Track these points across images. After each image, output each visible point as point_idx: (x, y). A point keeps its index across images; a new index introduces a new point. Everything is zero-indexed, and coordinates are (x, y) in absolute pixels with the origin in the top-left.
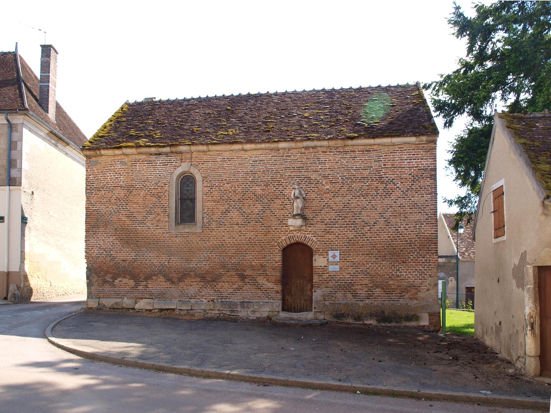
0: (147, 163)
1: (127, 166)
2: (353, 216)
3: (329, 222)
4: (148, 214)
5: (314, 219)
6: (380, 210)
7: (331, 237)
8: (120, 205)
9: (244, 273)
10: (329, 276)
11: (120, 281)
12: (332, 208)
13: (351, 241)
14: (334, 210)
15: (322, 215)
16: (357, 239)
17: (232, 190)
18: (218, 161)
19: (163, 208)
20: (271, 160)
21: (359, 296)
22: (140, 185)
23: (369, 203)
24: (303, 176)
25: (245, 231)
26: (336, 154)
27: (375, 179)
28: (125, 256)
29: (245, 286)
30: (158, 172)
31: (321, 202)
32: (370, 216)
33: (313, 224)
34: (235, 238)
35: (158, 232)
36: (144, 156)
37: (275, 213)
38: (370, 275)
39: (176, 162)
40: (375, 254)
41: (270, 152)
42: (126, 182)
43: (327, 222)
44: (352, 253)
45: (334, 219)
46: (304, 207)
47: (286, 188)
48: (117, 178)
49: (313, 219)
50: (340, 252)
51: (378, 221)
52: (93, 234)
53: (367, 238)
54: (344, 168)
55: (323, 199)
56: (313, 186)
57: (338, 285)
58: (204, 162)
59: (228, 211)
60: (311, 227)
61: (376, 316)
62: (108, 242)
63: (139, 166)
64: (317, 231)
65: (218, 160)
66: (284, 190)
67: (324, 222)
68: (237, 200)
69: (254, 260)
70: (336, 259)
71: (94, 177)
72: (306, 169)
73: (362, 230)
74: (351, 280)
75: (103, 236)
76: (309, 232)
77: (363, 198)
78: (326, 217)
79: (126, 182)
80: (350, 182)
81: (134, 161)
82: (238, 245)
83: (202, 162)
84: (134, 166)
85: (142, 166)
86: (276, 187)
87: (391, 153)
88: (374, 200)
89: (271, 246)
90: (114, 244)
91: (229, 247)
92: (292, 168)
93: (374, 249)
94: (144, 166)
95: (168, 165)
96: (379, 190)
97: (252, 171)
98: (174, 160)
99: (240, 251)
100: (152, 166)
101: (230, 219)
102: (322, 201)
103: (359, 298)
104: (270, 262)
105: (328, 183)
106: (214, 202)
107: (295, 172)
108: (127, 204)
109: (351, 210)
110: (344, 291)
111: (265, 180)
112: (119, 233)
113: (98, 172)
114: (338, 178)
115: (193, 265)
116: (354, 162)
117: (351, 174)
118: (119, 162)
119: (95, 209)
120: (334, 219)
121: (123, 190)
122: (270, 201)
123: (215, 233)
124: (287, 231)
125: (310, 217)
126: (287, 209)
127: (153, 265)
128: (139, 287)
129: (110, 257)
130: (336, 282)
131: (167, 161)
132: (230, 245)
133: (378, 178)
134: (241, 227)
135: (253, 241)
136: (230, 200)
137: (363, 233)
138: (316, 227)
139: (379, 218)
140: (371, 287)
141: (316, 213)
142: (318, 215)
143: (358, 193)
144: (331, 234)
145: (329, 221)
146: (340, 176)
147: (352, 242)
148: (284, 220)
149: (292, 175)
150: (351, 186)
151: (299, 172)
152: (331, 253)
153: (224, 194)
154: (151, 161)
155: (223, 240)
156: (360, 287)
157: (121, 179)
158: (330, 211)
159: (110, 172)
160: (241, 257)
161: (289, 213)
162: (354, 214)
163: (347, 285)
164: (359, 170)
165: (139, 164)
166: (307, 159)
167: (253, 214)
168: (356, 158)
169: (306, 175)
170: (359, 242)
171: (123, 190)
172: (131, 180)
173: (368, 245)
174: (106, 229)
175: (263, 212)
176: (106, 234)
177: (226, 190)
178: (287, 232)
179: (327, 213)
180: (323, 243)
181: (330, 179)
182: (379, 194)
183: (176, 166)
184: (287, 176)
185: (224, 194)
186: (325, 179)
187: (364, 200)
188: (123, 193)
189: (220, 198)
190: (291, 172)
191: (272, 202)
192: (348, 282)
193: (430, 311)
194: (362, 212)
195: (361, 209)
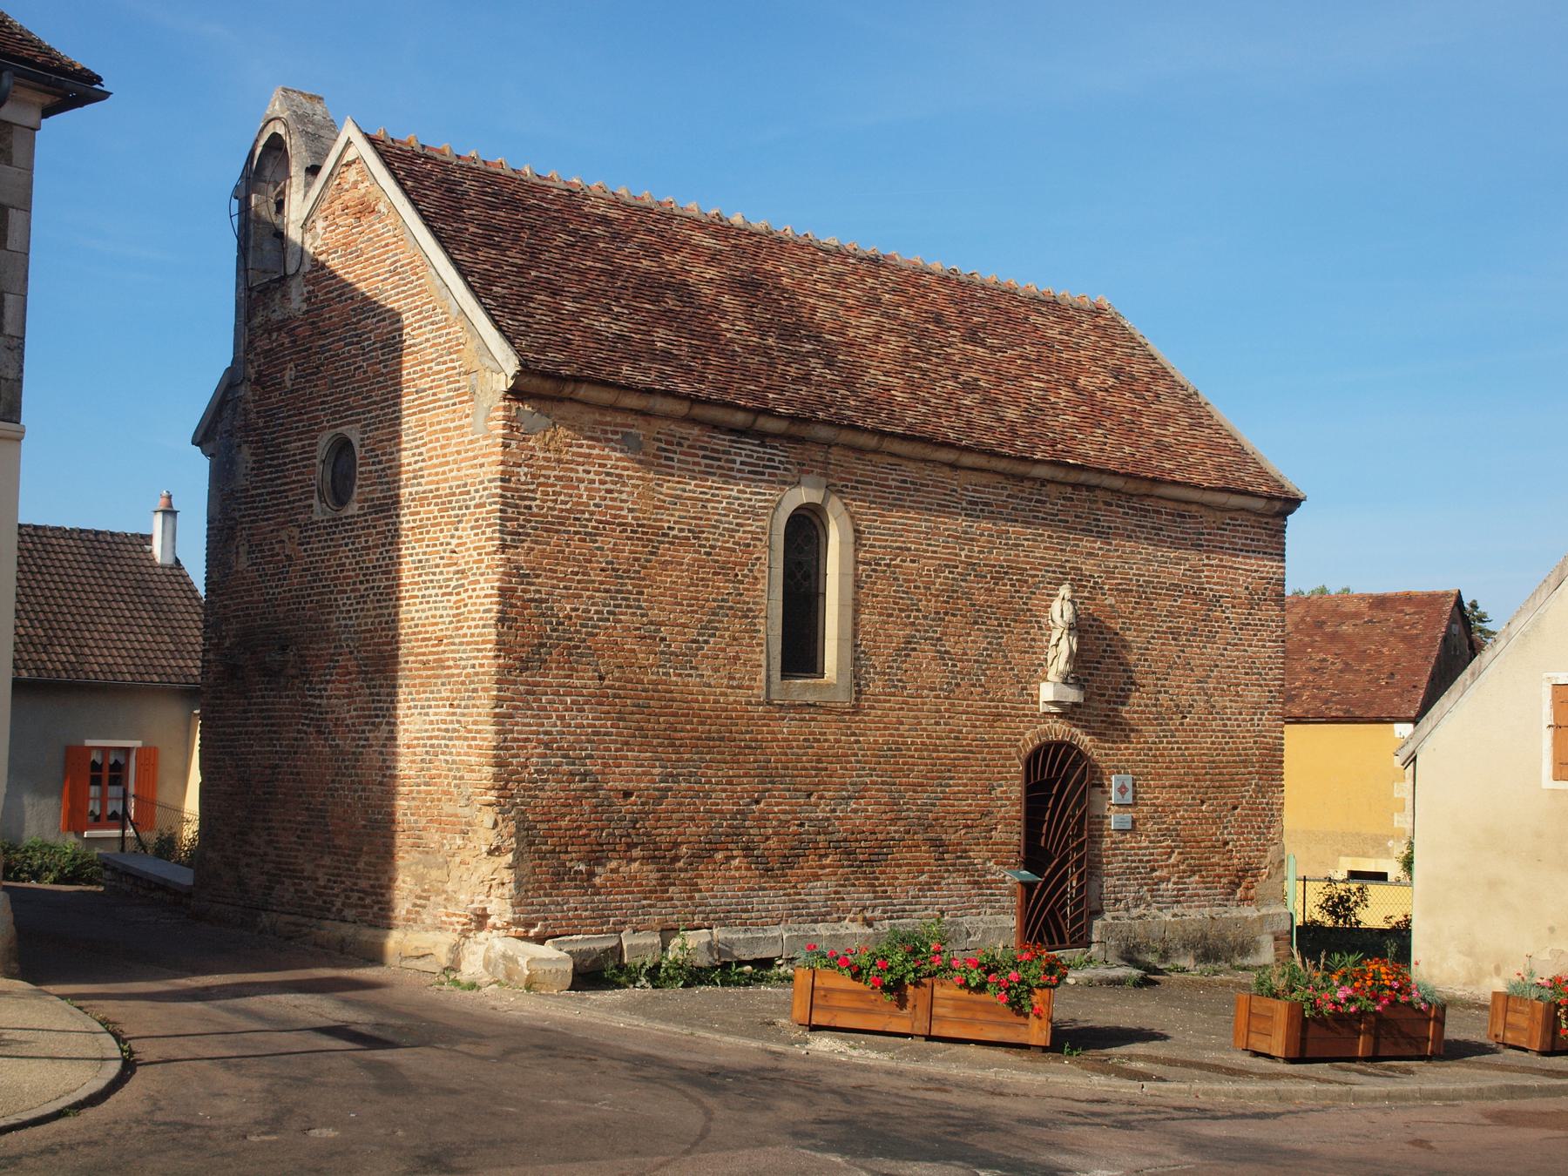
0: (704, 457)
1: (645, 454)
4: (703, 635)
6: (1199, 672)
7: (1118, 736)
8: (617, 592)
9: (944, 836)
11: (612, 871)
17: (923, 582)
18: (890, 487)
19: (747, 617)
20: (1007, 508)
22: (681, 530)
24: (1067, 564)
26: (1127, 514)
28: (631, 781)
29: (946, 875)
30: (734, 494)
31: (1098, 639)
34: (925, 730)
35: (731, 699)
36: (696, 431)
39: (786, 469)
41: (1005, 483)
42: (641, 510)
48: (609, 491)
52: (528, 692)
56: (1086, 594)
57: (1128, 868)
58: (857, 482)
59: (907, 648)
61: (1194, 947)
62: (577, 726)
63: (679, 461)
65: (890, 483)
67: (1104, 695)
71: (534, 476)
75: (561, 702)
79: (641, 510)
81: (667, 443)
83: (851, 481)
84: (667, 458)
85: (688, 463)
87: (1219, 529)
90: (596, 733)
91: (913, 757)
94: (695, 464)
95: (763, 474)
97: (966, 533)
98: (780, 462)
99: (937, 771)
100: (719, 467)
101: (916, 669)
106: (880, 614)
107: (1053, 549)
108: (642, 593)
112: (615, 696)
113: (545, 459)
115: (824, 811)
116: (1159, 541)
118: (619, 437)
119: (532, 596)
121: (628, 538)
123: (880, 712)
127: (717, 812)
128: (671, 889)
129: (581, 781)
131: (763, 459)
132: (916, 750)
135: (965, 742)
136: (918, 610)
137: (1171, 731)
140: (1184, 872)
141: (1090, 668)
143: (1165, 625)
151: (1061, 550)
152: (1114, 781)
153: (904, 592)
154: (717, 451)
155: (900, 736)
157: (624, 496)
159: (587, 467)
165: (681, 453)
166: (1076, 516)
168: (1161, 529)
171: (628, 538)
172: (656, 507)
174: (570, 676)
176: (570, 694)
183: (785, 483)
185: (904, 592)
188: (631, 552)
189: (895, 603)
190: (1045, 548)
193: (1275, 929)
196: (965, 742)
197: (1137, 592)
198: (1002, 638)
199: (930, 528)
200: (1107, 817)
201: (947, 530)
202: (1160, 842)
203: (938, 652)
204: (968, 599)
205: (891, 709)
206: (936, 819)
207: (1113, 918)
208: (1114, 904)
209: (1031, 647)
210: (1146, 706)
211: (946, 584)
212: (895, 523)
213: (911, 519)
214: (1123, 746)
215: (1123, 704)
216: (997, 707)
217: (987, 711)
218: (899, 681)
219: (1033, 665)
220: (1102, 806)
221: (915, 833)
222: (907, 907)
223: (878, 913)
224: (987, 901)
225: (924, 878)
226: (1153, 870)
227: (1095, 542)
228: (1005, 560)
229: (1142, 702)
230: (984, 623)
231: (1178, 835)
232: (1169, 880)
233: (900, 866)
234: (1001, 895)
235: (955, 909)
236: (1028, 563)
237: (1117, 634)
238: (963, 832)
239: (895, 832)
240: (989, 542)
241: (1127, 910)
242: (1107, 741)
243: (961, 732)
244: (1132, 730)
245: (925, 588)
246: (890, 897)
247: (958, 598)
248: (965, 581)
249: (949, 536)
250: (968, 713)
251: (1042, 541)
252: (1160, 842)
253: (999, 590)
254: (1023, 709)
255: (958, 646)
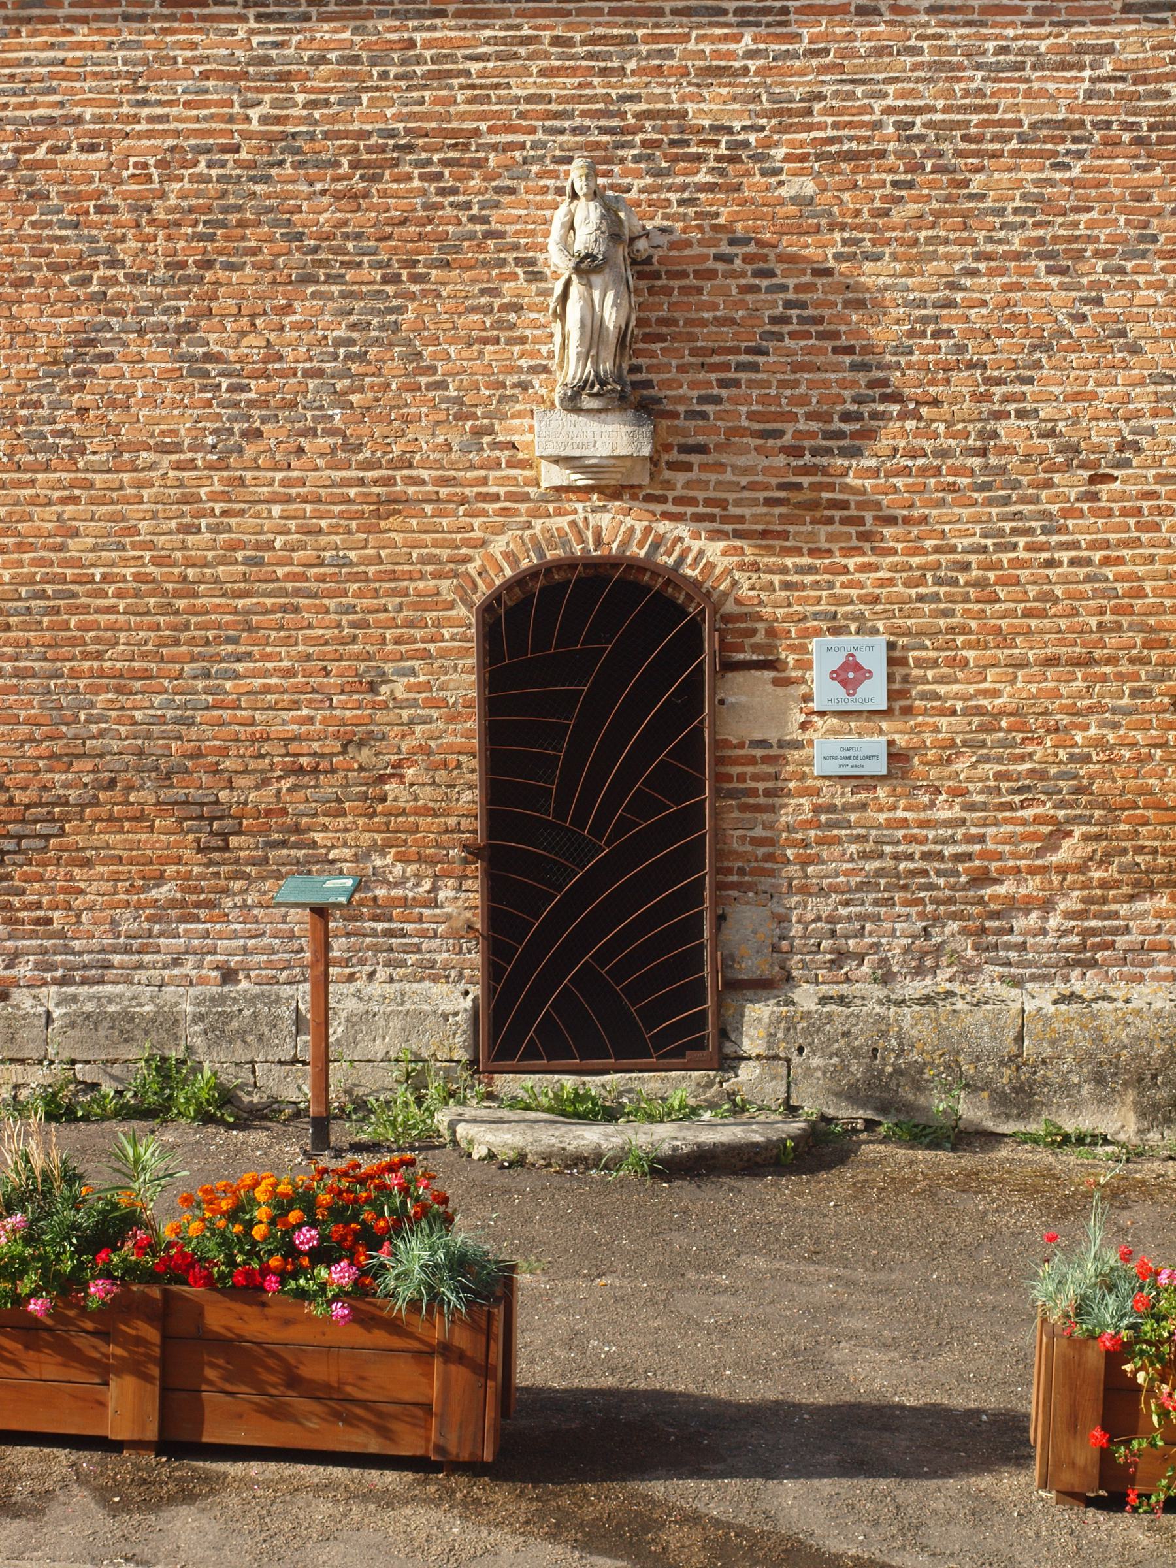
2: (978, 398)
3: (811, 435)
5: (709, 409)
7: (831, 538)
9: (223, 795)
10: (817, 810)
12: (836, 335)
13: (966, 567)
14: (850, 350)
15: (766, 384)
16: (1005, 557)
21: (1023, 947)
23: (1085, 301)
24: (628, 107)
25: (224, 496)
27: (1126, 137)
29: (237, 885)
32: (1094, 396)
33: (701, 449)
34: (151, 546)
37: (433, 370)
38: (1092, 805)
40: (1132, 661)
43: (798, 434)
44: (971, 654)
45: (846, 417)
46: (641, 322)
47: (512, 191)
49: (703, 415)
50: (891, 646)
51: (1151, 431)
53: (1075, 546)
54: (919, 51)
55: (770, 274)
56: (702, 178)
57: (879, 873)
60: (688, 467)
61: (1142, 1081)
64: (731, 496)
66: (497, 205)
67: (780, 434)
68: (161, 273)
69: (296, 705)
70: (863, 690)
72: (649, 56)
73: (1044, 494)
74: (969, 839)
76: (678, 501)
77: (1050, 271)
78: (792, 401)
80: (959, 154)
82: (177, 595)
86: (439, 176)
88: (1122, 285)
89: (415, 606)
91: (111, 610)
92: (556, 41)
93: (1119, 627)
96: (1159, 213)
97: (266, 61)
99: (191, 642)
101: (113, 404)
102: (765, 283)
103: (1021, 964)
104: (406, 714)
105: (804, 158)
107: (573, 71)
109: (961, 349)
110: (922, 916)
111: (356, 127)
114: (878, 125)
117: (966, 93)
120: (846, 417)
122: (396, 279)
124: (525, 498)
125: (682, 399)
126: (522, 340)
130: (865, 856)
132: (120, 595)
133: (1152, 127)
134: (191, 465)
135: (280, 571)
136: (114, 264)
137: (1046, 515)
138: (720, 467)
139: (1155, 416)
140: (1104, 884)
141: (725, 367)
142: (736, 383)
143: (1017, 238)
144: (830, 521)
145: (815, 426)
146: (889, 111)
147: (975, 573)
148: (504, 418)
149: (554, 92)
150: (966, 183)
151: (604, 72)
153: (63, 224)
156: (1032, 886)
158: (819, 360)
160: (200, 684)
161: (533, 370)
162: (988, 381)
163: (939, 873)
164: (1020, 67)
167: (282, 374)
169: (651, 98)
170: (1024, 574)
173: (1083, 597)
175: (349, 357)
177: (80, 197)
178: (523, 507)
179: (798, 368)
180: (776, 579)
181: (822, 126)
182: (1154, 239)
184: (517, 100)
185: (63, 224)
186: (783, 129)
187: (1054, 281)
190: (542, 73)
191: (415, 288)
192: (948, 850)
194: (1038, 365)
195: (1034, 348)
196: (280, 571)
197: (899, 155)
198: (400, 310)
199: (145, 61)
200: (797, 745)
201: (199, 61)
202: (1010, 807)
203: (182, 358)
204: (275, 224)
205: (33, 502)
206: (197, 755)
207: (824, 1000)
208: (835, 964)
209: (500, 325)
210: (943, 454)
211: (198, 194)
212: (27, 62)
213: (79, 46)
214: (852, 562)
215: (854, 452)
216: (389, 481)
217: (352, 492)
218: (62, 434)
219: (520, 369)
220: (780, 718)
221: (130, 788)
222: (116, 959)
223: (24, 970)
224: (376, 949)
225: (160, 893)
226: (982, 878)
227: (738, 38)
228: (399, 117)
229: (928, 445)
230: (339, 279)
231: (1079, 790)
232: (1047, 906)
233: (87, 863)
234: (423, 934)
235: (269, 965)
236: (482, 116)
237: (828, 272)
238: (286, 784)
239: (66, 785)
240: (343, 76)
241: (886, 978)
242: (798, 551)
243: (269, 546)
244: (891, 521)
245: (133, 209)
246: (62, 935)
247: (242, 224)
248: (266, 179)
249: (205, 75)
250: (288, 500)
251: (530, 57)
252: (1010, 807)
253: (384, 194)
254: (484, 482)
255: (251, 339)
